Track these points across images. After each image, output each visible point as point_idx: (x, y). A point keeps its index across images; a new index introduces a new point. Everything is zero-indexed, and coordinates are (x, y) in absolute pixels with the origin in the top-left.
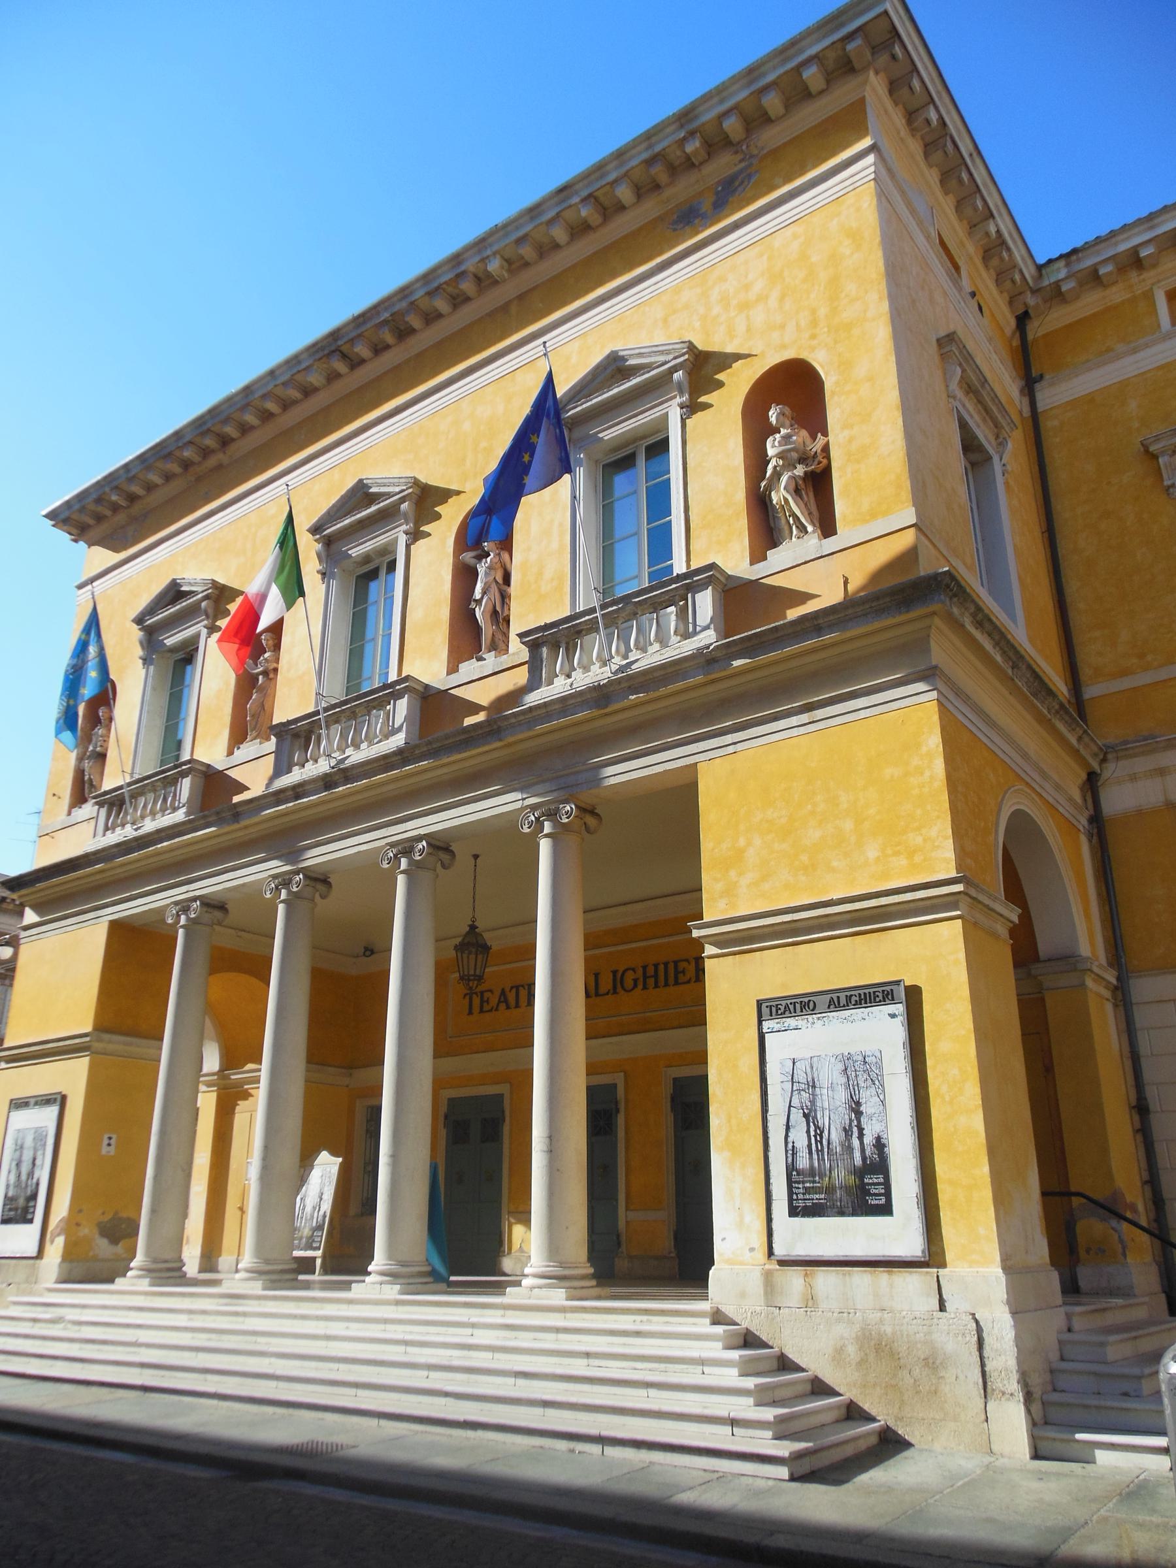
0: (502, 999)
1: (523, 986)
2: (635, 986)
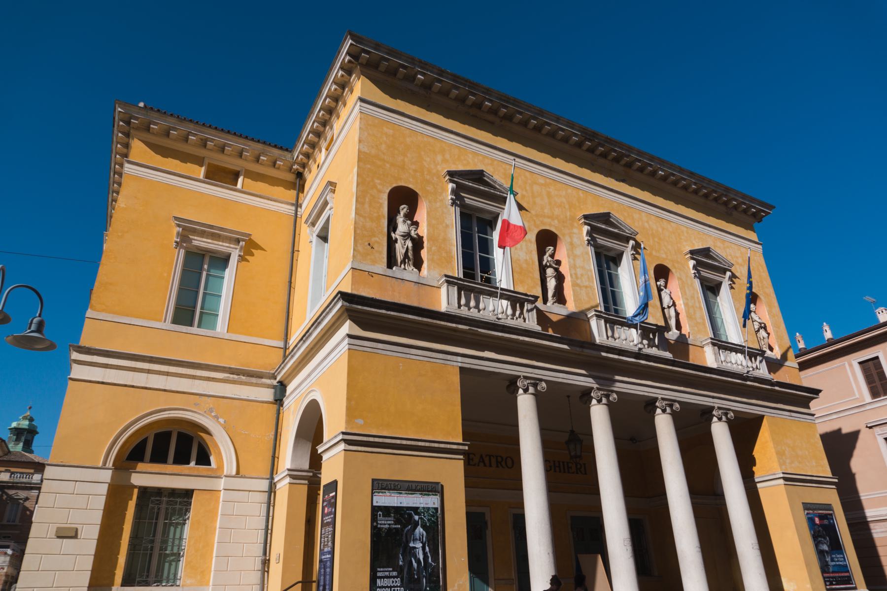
0: (481, 460)
1: (493, 456)
2: (551, 470)
